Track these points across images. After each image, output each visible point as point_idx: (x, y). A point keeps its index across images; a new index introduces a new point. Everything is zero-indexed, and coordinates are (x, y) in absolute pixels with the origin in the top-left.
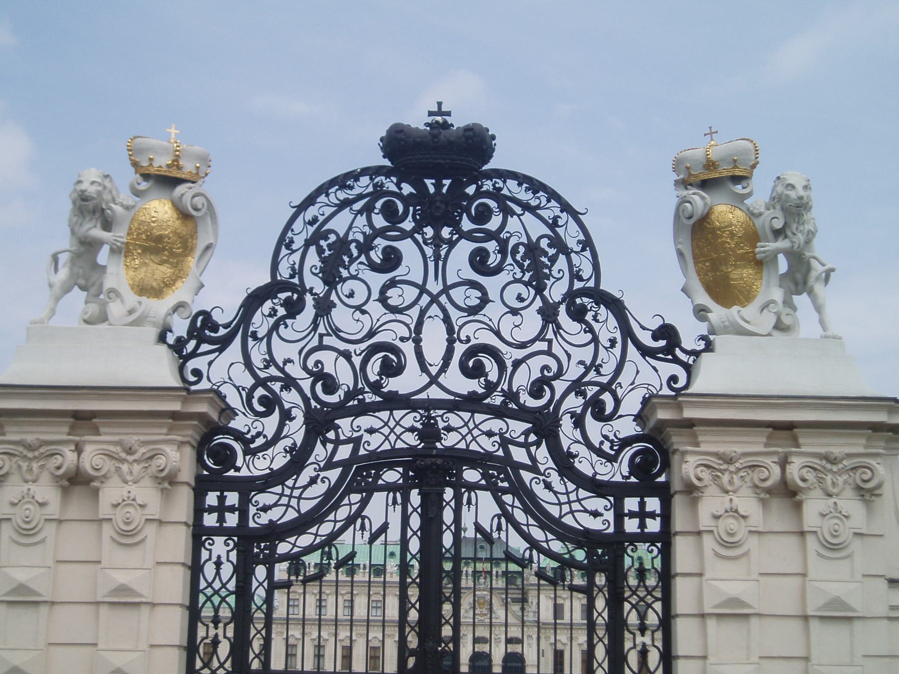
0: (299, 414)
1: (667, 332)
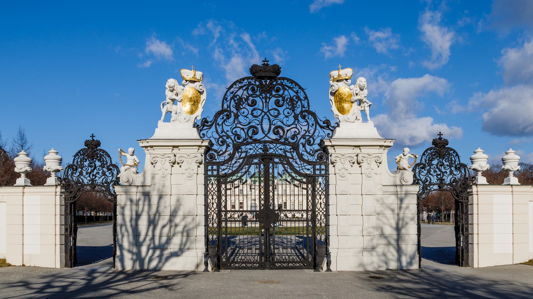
0: (231, 145)
1: (327, 122)
